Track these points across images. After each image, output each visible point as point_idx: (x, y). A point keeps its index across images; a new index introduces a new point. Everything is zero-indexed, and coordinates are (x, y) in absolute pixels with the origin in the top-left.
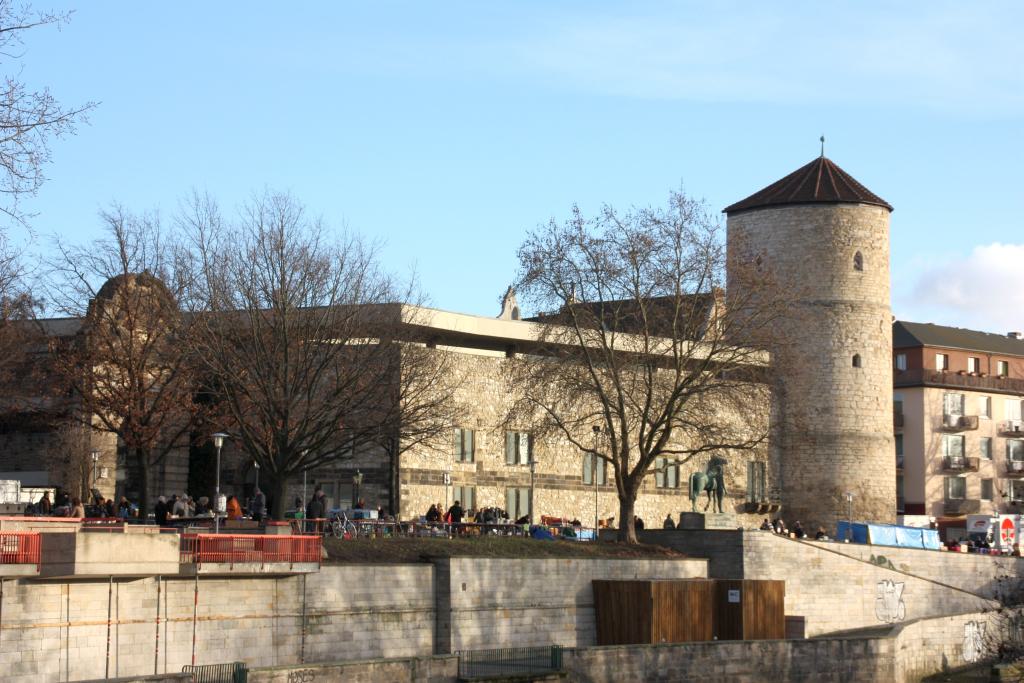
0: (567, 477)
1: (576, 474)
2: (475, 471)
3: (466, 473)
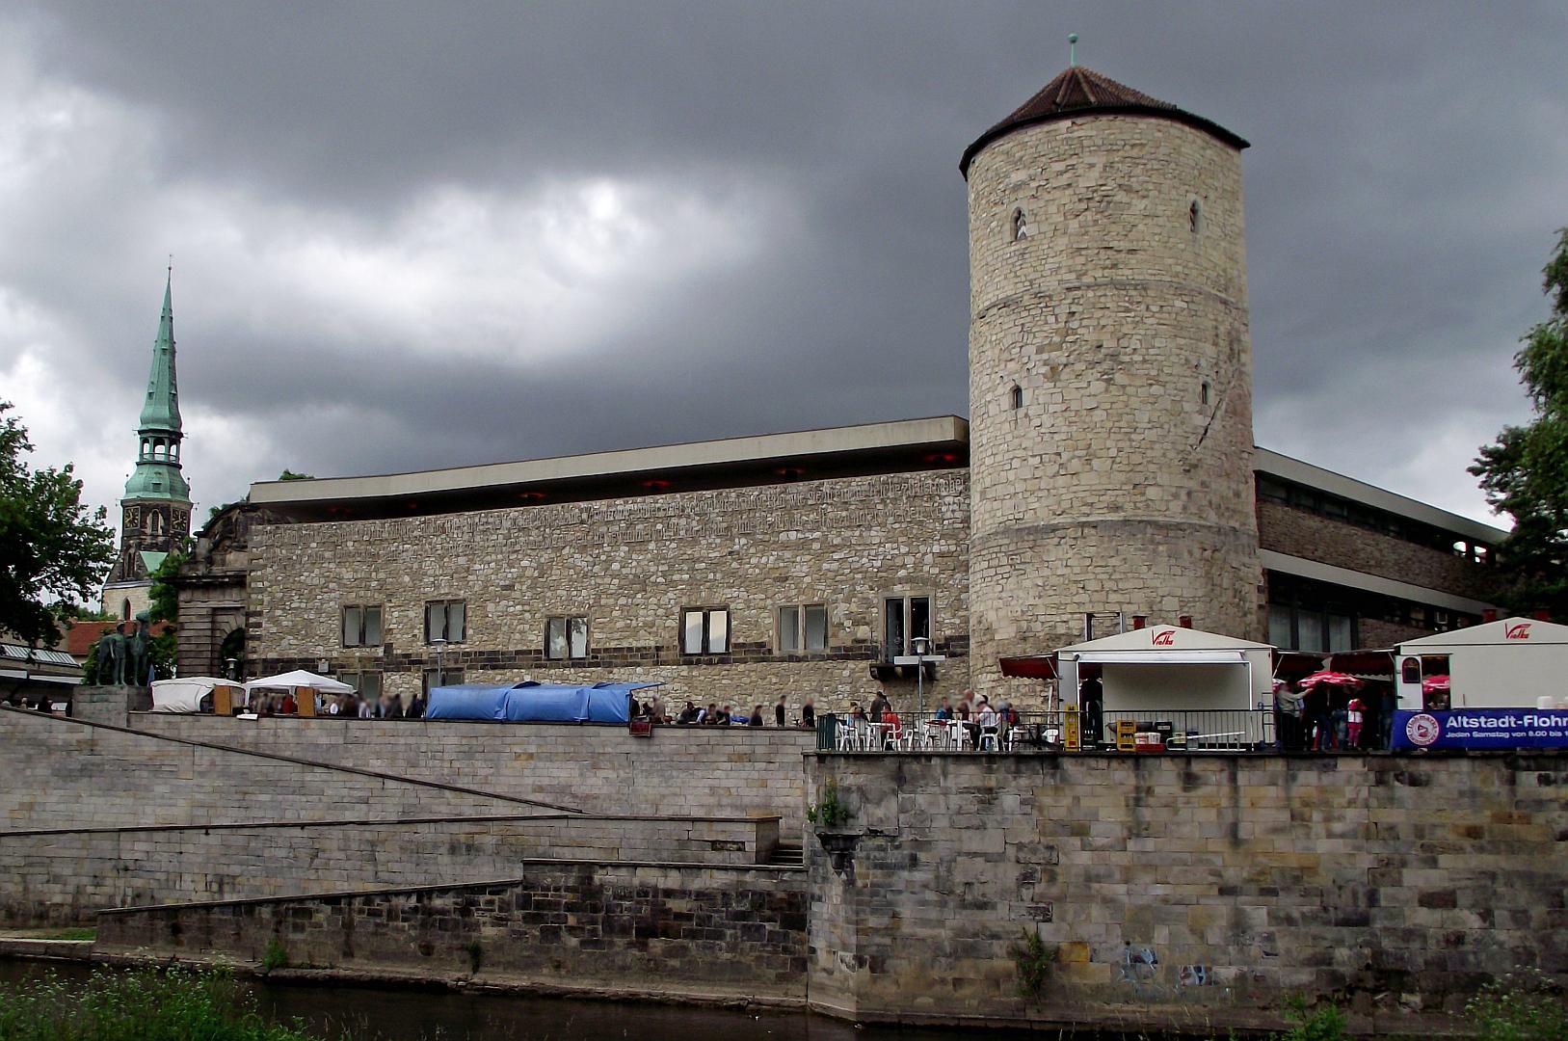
0: (518, 652)
1: (533, 647)
2: (381, 654)
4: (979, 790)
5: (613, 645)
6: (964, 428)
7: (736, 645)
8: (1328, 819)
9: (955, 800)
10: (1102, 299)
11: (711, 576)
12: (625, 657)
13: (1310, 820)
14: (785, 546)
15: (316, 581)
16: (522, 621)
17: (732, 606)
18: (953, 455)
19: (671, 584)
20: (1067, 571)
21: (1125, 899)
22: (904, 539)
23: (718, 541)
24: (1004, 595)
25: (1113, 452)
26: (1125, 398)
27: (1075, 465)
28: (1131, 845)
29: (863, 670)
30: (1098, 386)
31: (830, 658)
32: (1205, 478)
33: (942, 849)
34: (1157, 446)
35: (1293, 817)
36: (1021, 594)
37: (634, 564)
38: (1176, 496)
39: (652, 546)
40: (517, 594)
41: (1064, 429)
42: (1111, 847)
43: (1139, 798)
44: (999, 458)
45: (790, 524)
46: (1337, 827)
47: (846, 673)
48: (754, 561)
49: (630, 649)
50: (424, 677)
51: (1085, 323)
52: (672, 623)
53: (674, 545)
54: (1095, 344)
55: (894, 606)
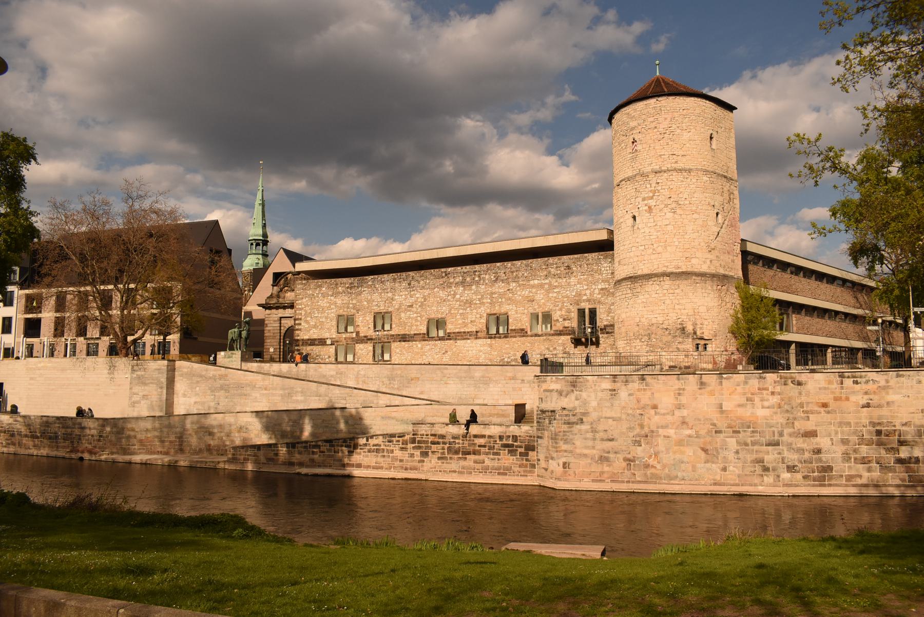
0: (415, 334)
1: (422, 332)
3: (345, 338)
4: (610, 390)
5: (457, 330)
6: (611, 232)
7: (511, 330)
8: (762, 400)
9: (600, 394)
10: (671, 177)
11: (500, 300)
12: (462, 336)
13: (754, 401)
14: (533, 286)
15: (325, 305)
16: (416, 321)
17: (509, 313)
18: (606, 246)
19: (483, 304)
20: (657, 295)
21: (674, 436)
22: (586, 283)
23: (503, 285)
24: (629, 306)
25: (677, 243)
26: (682, 220)
27: (660, 249)
28: (677, 413)
29: (568, 340)
30: (669, 215)
31: (553, 335)
32: (718, 254)
33: (594, 415)
34: (696, 240)
35: (747, 400)
36: (636, 306)
37: (466, 295)
38: (704, 262)
39: (474, 287)
40: (414, 309)
41: (655, 233)
42: (668, 414)
43: (679, 393)
44: (626, 247)
45: (534, 277)
46: (766, 404)
47: (560, 342)
48: (519, 293)
49: (464, 332)
50: (374, 346)
51: (663, 187)
52: (484, 321)
53: (483, 287)
54: (669, 196)
55: (581, 312)
